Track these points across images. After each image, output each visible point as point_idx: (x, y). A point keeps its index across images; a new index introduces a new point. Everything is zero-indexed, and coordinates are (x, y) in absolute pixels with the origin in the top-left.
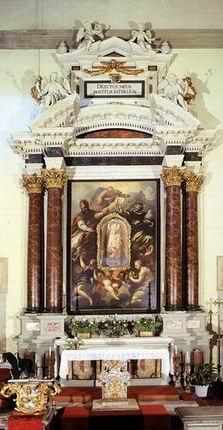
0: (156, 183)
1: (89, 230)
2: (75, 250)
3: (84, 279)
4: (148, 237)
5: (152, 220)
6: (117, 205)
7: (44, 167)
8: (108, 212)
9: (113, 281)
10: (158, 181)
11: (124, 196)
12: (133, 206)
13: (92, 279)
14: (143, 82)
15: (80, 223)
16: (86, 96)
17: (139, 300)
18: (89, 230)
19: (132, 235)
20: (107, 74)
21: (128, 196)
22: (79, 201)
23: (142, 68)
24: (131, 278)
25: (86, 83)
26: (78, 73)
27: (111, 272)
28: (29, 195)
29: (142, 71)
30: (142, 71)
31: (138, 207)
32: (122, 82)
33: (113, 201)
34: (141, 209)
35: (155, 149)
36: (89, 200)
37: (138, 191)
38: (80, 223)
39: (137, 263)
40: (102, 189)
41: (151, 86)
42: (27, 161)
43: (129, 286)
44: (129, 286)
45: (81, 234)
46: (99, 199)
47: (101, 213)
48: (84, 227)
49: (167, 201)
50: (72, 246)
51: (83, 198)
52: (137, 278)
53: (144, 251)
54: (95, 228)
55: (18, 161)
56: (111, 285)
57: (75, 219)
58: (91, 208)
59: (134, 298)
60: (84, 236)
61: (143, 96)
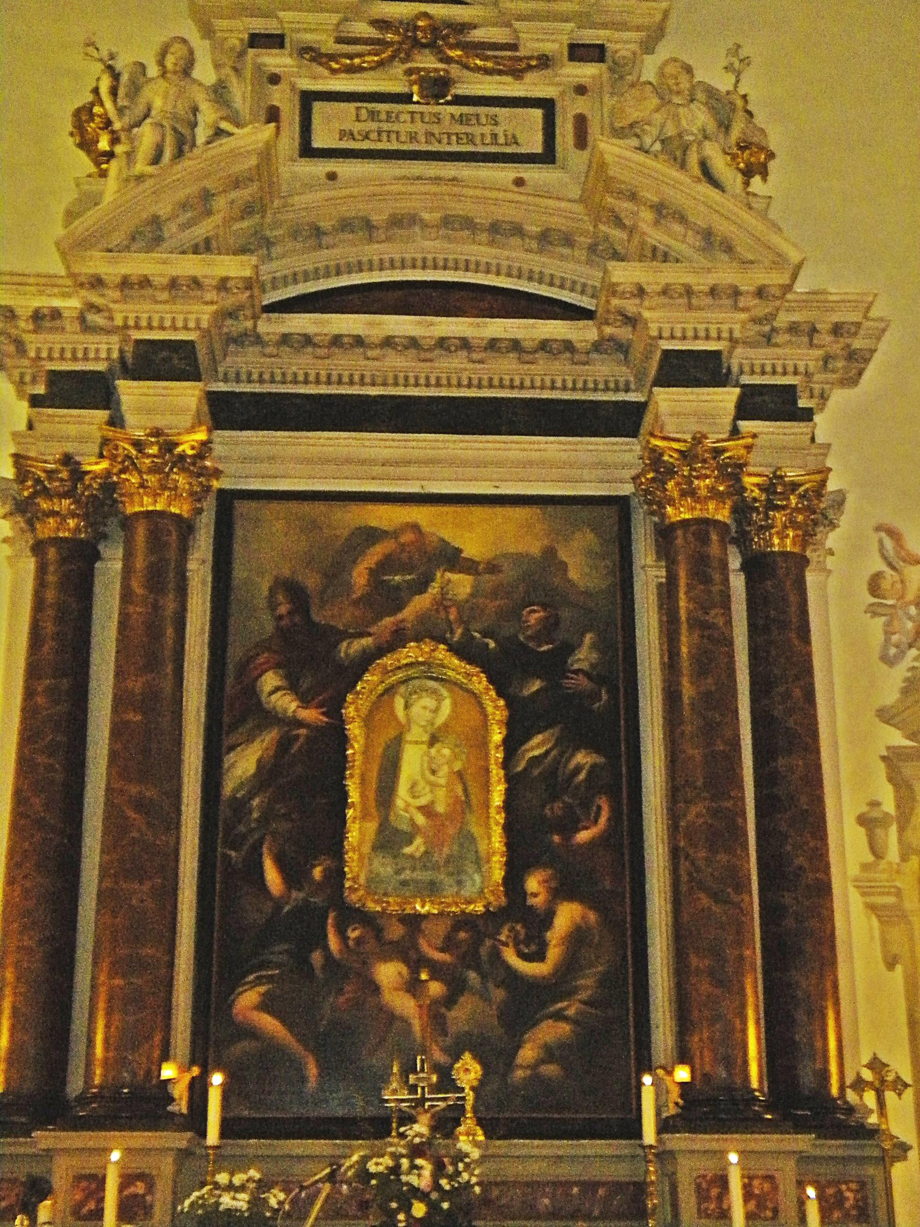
0: (610, 514)
1: (310, 715)
2: (239, 806)
3: (279, 951)
4: (582, 758)
5: (598, 676)
6: (442, 603)
7: (116, 421)
8: (398, 639)
9: (416, 963)
10: (621, 504)
11: (469, 567)
12: (514, 613)
13: (317, 958)
14: (548, 106)
15: (270, 680)
16: (307, 151)
17: (551, 1070)
18: (310, 715)
19: (511, 745)
20: (398, 69)
21: (493, 568)
22: (266, 593)
23: (549, 47)
24: (511, 957)
25: (308, 99)
26: (275, 61)
27: (414, 922)
28: (38, 548)
29: (545, 62)
30: (545, 62)
31: (534, 617)
32: (459, 100)
33: (421, 586)
34: (550, 626)
35: (624, 373)
36: (311, 581)
37: (534, 547)
38: (270, 680)
39: (533, 883)
40: (371, 535)
41: (581, 122)
42: (36, 401)
43: (499, 994)
44: (499, 994)
45: (267, 740)
46: (360, 576)
47: (366, 642)
48: (287, 704)
49: (668, 592)
50: (228, 787)
51: (286, 572)
52: (539, 956)
53: (570, 826)
54: (335, 708)
55: (25, 404)
56: (413, 987)
57: (243, 667)
58: (316, 617)
59: (527, 1054)
60: (283, 745)
61: (548, 156)
